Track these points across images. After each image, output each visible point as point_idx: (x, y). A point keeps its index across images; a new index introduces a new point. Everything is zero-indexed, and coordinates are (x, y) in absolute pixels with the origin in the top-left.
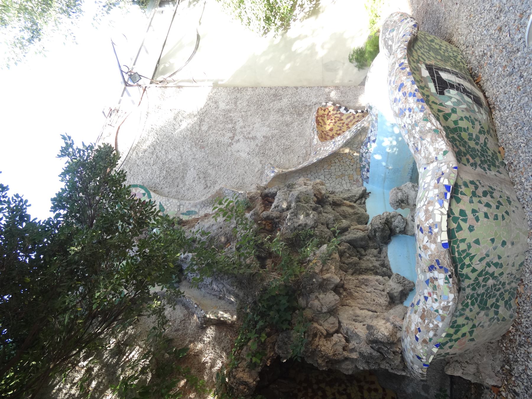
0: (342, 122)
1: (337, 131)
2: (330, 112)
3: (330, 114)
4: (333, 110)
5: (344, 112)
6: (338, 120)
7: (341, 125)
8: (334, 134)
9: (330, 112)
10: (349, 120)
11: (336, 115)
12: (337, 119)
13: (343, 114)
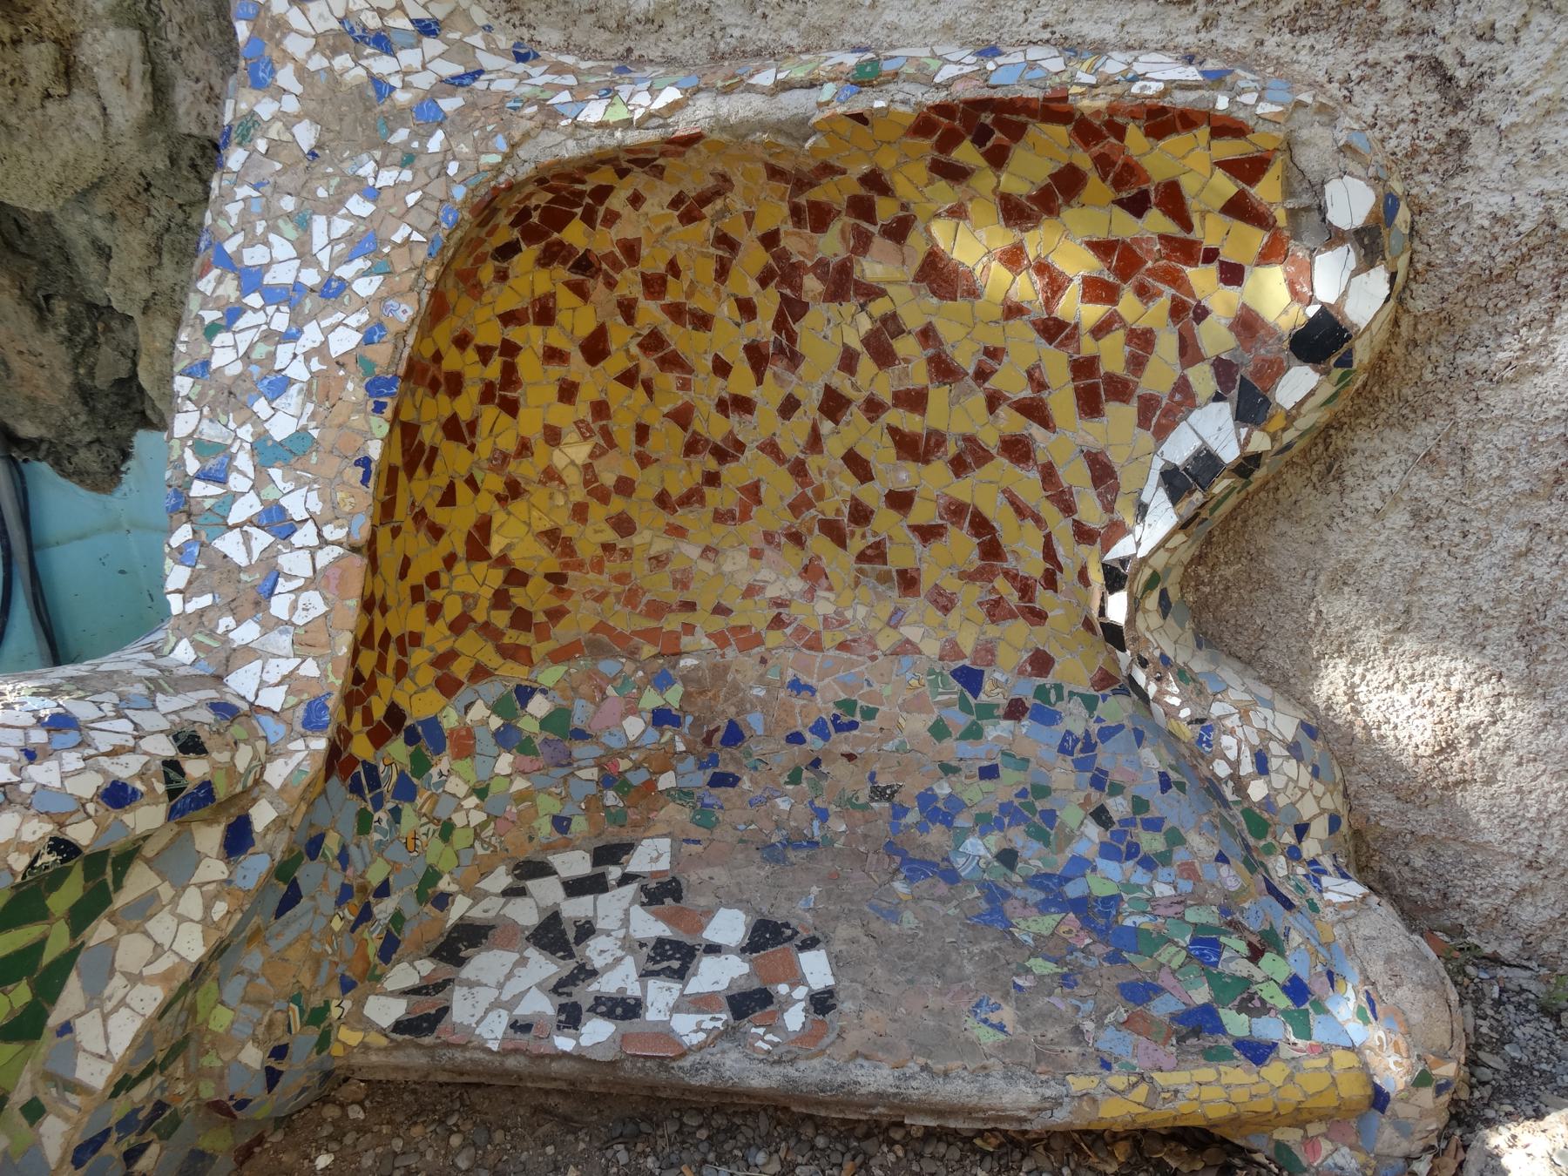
0: (1061, 401)
1: (927, 335)
2: (1232, 274)
3: (1201, 278)
4: (1247, 324)
5: (1180, 448)
6: (1084, 368)
7: (1011, 381)
8: (879, 307)
9: (1232, 274)
10: (1076, 475)
11: (1167, 344)
12: (1112, 355)
13: (1162, 433)
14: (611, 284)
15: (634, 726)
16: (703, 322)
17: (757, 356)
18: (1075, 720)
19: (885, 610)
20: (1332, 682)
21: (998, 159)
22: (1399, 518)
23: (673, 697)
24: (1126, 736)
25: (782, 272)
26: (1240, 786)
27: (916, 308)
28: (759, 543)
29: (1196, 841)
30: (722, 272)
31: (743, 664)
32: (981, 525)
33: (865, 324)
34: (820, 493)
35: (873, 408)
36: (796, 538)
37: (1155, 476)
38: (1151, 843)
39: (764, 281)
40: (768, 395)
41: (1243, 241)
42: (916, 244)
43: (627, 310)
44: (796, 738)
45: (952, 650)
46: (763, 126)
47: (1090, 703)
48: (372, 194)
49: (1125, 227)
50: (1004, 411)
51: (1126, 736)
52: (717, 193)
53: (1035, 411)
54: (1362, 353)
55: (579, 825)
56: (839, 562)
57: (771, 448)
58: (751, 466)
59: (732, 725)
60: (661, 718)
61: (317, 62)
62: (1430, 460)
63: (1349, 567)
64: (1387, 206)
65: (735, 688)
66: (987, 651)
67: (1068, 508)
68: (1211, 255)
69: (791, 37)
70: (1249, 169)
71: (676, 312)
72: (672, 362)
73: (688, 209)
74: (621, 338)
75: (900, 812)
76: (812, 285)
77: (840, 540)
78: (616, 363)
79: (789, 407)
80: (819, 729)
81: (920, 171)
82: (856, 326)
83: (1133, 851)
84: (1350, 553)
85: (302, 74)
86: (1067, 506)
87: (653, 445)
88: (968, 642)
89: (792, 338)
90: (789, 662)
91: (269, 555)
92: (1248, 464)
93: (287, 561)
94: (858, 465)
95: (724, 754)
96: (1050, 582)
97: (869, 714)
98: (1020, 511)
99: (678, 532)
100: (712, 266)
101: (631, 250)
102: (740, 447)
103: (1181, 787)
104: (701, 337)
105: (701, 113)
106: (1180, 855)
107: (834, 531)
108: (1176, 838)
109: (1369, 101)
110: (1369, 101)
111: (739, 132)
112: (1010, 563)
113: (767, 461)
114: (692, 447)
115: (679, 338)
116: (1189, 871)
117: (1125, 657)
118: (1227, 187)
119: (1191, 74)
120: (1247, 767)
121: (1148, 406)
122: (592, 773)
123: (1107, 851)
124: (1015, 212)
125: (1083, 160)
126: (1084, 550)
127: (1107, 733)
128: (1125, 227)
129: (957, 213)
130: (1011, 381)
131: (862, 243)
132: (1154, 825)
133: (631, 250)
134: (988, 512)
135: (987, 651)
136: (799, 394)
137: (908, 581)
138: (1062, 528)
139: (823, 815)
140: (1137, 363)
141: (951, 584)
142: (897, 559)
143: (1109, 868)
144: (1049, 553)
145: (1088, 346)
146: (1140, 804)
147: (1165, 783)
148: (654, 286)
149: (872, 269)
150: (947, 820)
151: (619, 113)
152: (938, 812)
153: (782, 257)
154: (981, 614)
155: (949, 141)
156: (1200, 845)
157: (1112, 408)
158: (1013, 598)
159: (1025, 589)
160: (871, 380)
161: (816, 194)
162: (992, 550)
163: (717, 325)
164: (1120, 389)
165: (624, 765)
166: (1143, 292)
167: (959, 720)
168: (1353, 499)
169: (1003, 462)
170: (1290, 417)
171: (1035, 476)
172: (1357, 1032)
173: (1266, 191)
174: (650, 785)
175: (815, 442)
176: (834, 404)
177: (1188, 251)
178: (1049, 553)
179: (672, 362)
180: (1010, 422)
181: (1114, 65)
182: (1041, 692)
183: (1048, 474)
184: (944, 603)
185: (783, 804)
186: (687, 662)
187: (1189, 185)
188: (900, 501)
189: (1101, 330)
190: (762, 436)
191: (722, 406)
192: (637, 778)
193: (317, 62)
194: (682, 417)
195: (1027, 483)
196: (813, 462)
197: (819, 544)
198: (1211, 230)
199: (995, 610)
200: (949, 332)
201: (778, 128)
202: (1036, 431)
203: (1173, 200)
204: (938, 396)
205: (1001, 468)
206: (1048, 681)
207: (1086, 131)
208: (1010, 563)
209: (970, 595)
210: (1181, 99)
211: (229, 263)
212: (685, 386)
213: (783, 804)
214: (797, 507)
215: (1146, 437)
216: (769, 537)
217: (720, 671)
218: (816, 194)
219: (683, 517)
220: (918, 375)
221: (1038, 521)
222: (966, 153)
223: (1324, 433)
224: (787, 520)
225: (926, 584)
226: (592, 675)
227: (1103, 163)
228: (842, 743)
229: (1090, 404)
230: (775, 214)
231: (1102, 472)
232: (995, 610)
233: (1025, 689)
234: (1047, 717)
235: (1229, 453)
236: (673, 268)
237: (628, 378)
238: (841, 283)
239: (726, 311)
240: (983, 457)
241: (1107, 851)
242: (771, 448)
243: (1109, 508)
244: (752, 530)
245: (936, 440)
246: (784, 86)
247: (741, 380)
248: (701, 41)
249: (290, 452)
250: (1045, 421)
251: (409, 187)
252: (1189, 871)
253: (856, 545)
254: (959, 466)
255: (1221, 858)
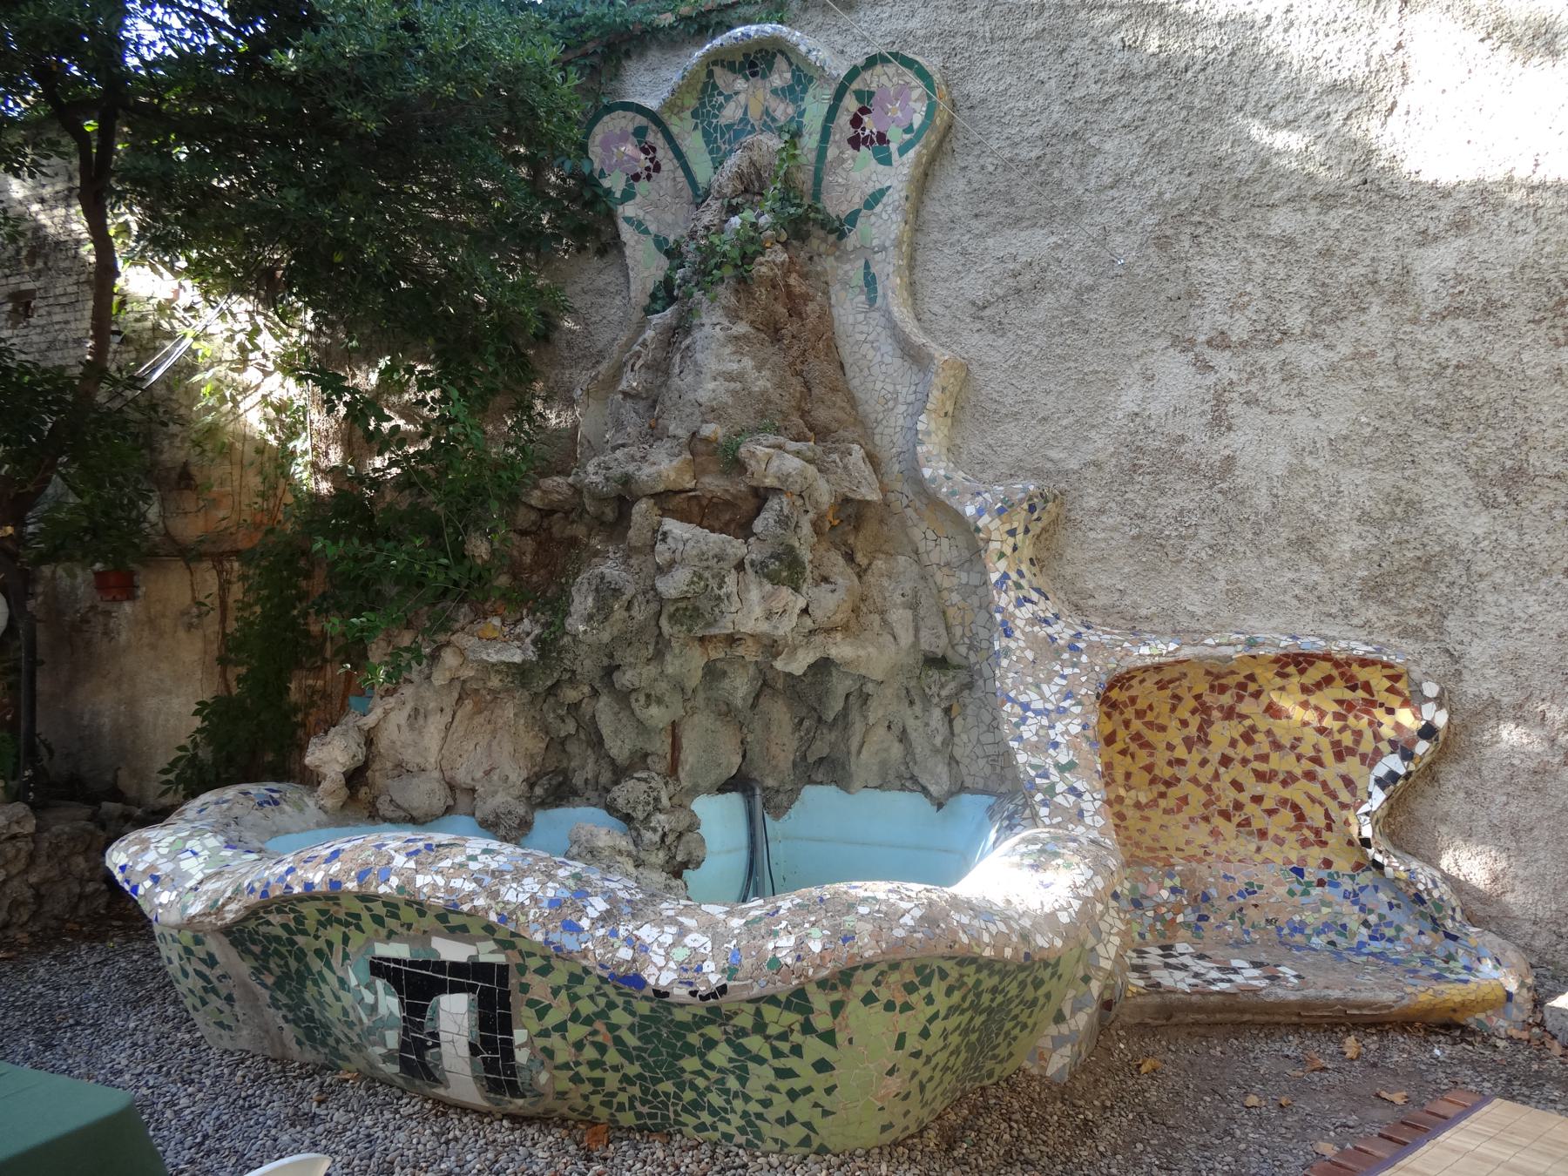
0: (1328, 756)
1: (1269, 733)
2: (1391, 711)
3: (1379, 713)
4: (1398, 727)
5: (1381, 770)
6: (1336, 744)
7: (1306, 749)
8: (1247, 723)
9: (1391, 711)
10: (1336, 785)
11: (1368, 734)
12: (1347, 739)
13: (1371, 766)
14: (1122, 713)
15: (1165, 894)
16: (1163, 728)
17: (1189, 743)
18: (1347, 885)
19: (1253, 847)
20: (1446, 862)
21: (1302, 672)
22: (1461, 795)
23: (1177, 881)
24: (1370, 890)
25: (1202, 709)
26: (1429, 894)
27: (1264, 723)
28: (1187, 822)
29: (1408, 928)
30: (1173, 709)
31: (1202, 870)
32: (1295, 807)
33: (1241, 729)
34: (1218, 799)
35: (1245, 761)
36: (1206, 819)
37: (1372, 782)
38: (1390, 932)
39: (1193, 712)
40: (1195, 757)
41: (1394, 701)
42: (1264, 700)
43: (1127, 724)
44: (1230, 898)
45: (1287, 861)
46: (1212, 657)
47: (1352, 878)
48: (1063, 677)
49: (1348, 695)
50: (1304, 761)
51: (1370, 890)
52: (1178, 679)
53: (1317, 760)
54: (1441, 738)
55: (1148, 936)
56: (1227, 828)
57: (1194, 780)
58: (1185, 788)
59: (1204, 894)
60: (1174, 890)
61: (1028, 629)
62: (1468, 774)
63: (1447, 813)
64: (1442, 690)
65: (1201, 879)
66: (1303, 860)
67: (1334, 796)
68: (1382, 705)
69: (1208, 627)
70: (1396, 678)
71: (1150, 725)
72: (1146, 745)
73: (1162, 686)
74: (1122, 734)
75: (1280, 929)
76: (1216, 714)
77: (1229, 819)
78: (1119, 746)
79: (1204, 762)
80: (1240, 894)
81: (1270, 675)
82: (1235, 729)
83: (1383, 936)
84: (1446, 808)
85: (1023, 632)
86: (1334, 796)
87: (1133, 781)
88: (1294, 857)
89: (1206, 735)
90: (1220, 869)
91: (1076, 805)
92: (1409, 774)
93: (1084, 805)
94: (1237, 786)
95: (1203, 906)
96: (1329, 828)
97: (1260, 887)
98: (1313, 800)
99: (1147, 819)
100: (1168, 707)
101: (1133, 700)
102: (1179, 780)
103: (1398, 906)
104: (1161, 735)
105: (1187, 652)
106: (1403, 935)
107: (1225, 815)
108: (1399, 929)
109: (1428, 660)
110: (1428, 660)
111: (1201, 660)
112: (1309, 822)
113: (1191, 786)
114: (1153, 782)
115: (1150, 735)
116: (1408, 941)
117: (1371, 852)
118: (1387, 684)
119: (1370, 649)
120: (1430, 886)
121: (1363, 757)
122: (1151, 914)
123: (1372, 938)
124: (1305, 689)
125: (1335, 673)
126: (1345, 812)
127: (1362, 889)
128: (1348, 695)
129: (1282, 689)
130: (1306, 749)
131: (1240, 698)
132: (1389, 924)
133: (1133, 700)
134: (1298, 802)
135: (1303, 860)
136: (1209, 757)
137: (1263, 834)
138: (1332, 806)
139: (1247, 933)
140: (1357, 742)
141: (1282, 834)
142: (1257, 824)
143: (1374, 943)
144: (1327, 815)
145: (1337, 737)
146: (1381, 917)
147: (1391, 906)
148: (1140, 714)
149: (1243, 708)
150: (1301, 931)
151: (1156, 652)
152: (1299, 928)
153: (1203, 704)
154: (1297, 846)
155: (1286, 665)
156: (1410, 929)
157: (1348, 759)
158: (1311, 836)
159: (1317, 832)
160: (1243, 749)
161: (1223, 681)
162: (1301, 817)
163: (1170, 730)
164: (1351, 752)
165: (1164, 910)
166: (1356, 717)
167: (1299, 889)
168: (1444, 788)
169: (1304, 781)
170: (1422, 758)
171: (1318, 786)
172: (1495, 974)
173: (1400, 685)
174: (1173, 920)
175: (1216, 776)
176: (1226, 761)
177: (1373, 704)
178: (1327, 815)
179: (1146, 745)
180: (1307, 765)
181: (1343, 644)
182: (1330, 875)
183: (1324, 785)
184: (1280, 841)
185: (1229, 928)
186: (1178, 868)
187: (1373, 683)
188: (1257, 799)
189: (1341, 731)
190: (1191, 774)
191: (1170, 763)
192: (1169, 916)
193: (1028, 629)
194: (1149, 768)
195: (1316, 789)
196: (1215, 785)
197: (1218, 821)
198: (1382, 696)
199: (1304, 843)
200: (1278, 732)
201: (1218, 659)
202: (1318, 768)
203: (1367, 687)
204: (1274, 756)
205: (1303, 784)
206: (1332, 870)
207: (1337, 664)
208: (1309, 822)
209: (1293, 836)
210: (1369, 656)
211: (1013, 701)
212: (1151, 755)
213: (1229, 928)
214: (1206, 805)
215: (1365, 768)
216: (1192, 819)
217: (1193, 872)
218: (1223, 681)
219: (1147, 812)
220: (1265, 748)
221: (1321, 804)
222: (1291, 669)
223: (1429, 766)
224: (1202, 810)
225: (1271, 834)
226: (1141, 873)
227: (1342, 675)
228: (1252, 900)
229: (1339, 756)
230: (1202, 687)
231: (1348, 782)
232: (1304, 843)
233: (1323, 874)
234: (1336, 885)
235: (1402, 771)
236: (1151, 707)
237: (1123, 752)
238: (1229, 713)
239: (1175, 724)
240: (1295, 779)
241: (1372, 938)
242: (1194, 780)
243: (1354, 795)
244: (1182, 817)
245: (1274, 774)
246: (1219, 645)
247: (1181, 752)
248: (1169, 626)
249: (1070, 767)
250: (1321, 765)
251: (1081, 675)
252: (1408, 941)
253: (1236, 820)
254: (1284, 783)
255: (1421, 933)
